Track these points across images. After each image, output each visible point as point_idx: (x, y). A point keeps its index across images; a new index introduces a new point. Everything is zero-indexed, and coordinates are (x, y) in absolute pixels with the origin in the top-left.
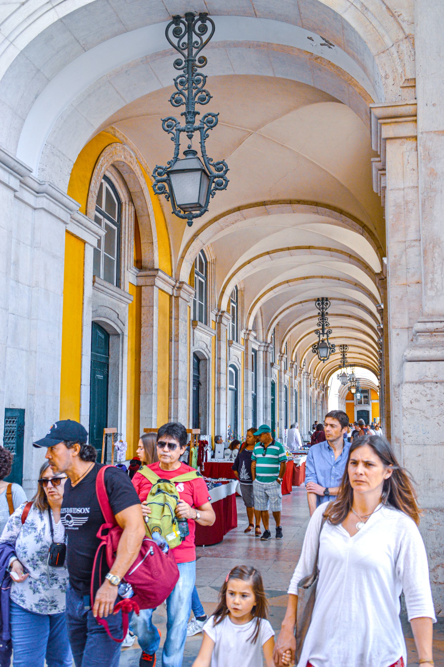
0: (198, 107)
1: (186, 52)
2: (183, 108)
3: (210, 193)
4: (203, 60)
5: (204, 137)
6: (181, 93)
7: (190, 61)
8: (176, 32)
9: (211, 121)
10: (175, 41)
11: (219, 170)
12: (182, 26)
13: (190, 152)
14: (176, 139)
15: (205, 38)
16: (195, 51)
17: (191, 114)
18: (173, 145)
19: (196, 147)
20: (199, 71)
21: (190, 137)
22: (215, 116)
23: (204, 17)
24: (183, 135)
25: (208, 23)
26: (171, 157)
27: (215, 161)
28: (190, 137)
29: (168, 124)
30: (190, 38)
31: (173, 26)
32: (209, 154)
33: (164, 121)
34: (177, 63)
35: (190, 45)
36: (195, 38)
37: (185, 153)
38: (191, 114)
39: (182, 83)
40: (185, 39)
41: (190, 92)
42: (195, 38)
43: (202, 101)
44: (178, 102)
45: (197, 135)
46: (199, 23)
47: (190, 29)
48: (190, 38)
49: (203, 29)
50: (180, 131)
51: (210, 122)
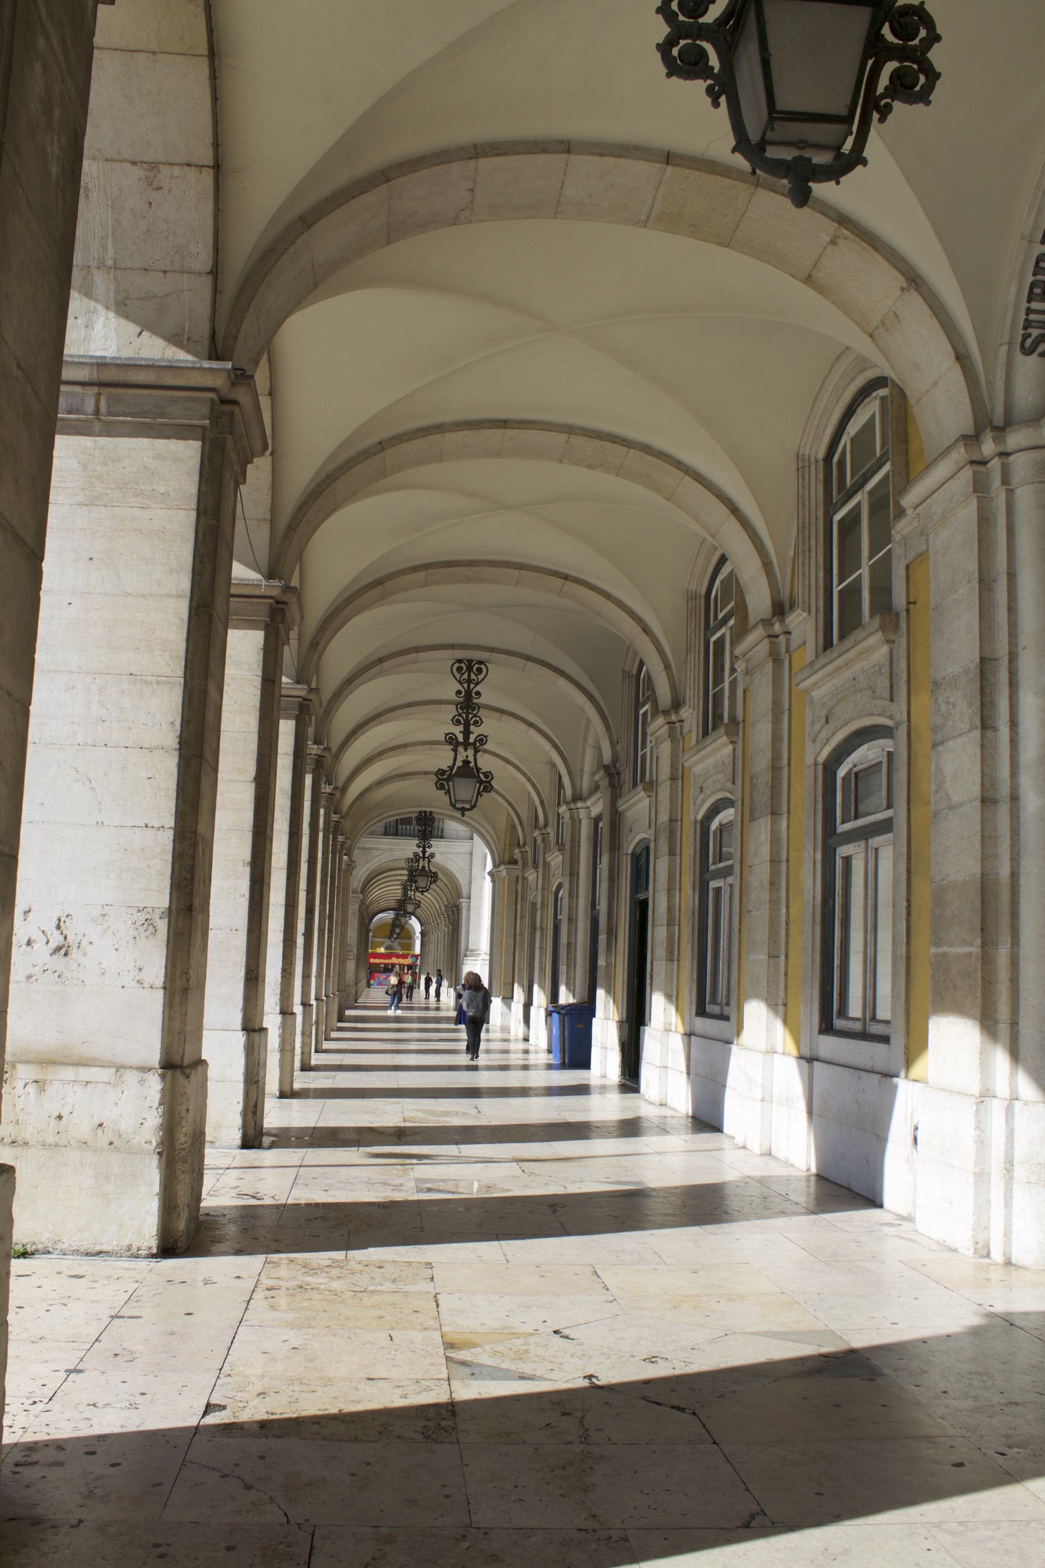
0: (472, 728)
1: (465, 685)
2: (461, 728)
4: (478, 693)
5: (476, 751)
6: (460, 715)
7: (468, 692)
8: (459, 669)
9: (482, 740)
10: (458, 676)
11: (486, 777)
12: (463, 665)
14: (455, 750)
15: (481, 677)
16: (472, 686)
17: (467, 733)
18: (452, 753)
19: (471, 758)
20: (475, 701)
21: (466, 750)
22: (486, 737)
23: (480, 662)
24: (461, 749)
25: (483, 666)
26: (450, 763)
27: (484, 770)
28: (466, 750)
29: (451, 740)
30: (469, 675)
31: (457, 665)
32: (479, 766)
33: (447, 735)
34: (459, 692)
35: (469, 681)
36: (473, 676)
38: (467, 733)
39: (462, 708)
40: (465, 676)
41: (467, 716)
42: (473, 676)
43: (476, 722)
44: (458, 722)
46: (477, 666)
47: (470, 669)
48: (469, 675)
49: (480, 671)
50: (458, 744)
51: (482, 740)
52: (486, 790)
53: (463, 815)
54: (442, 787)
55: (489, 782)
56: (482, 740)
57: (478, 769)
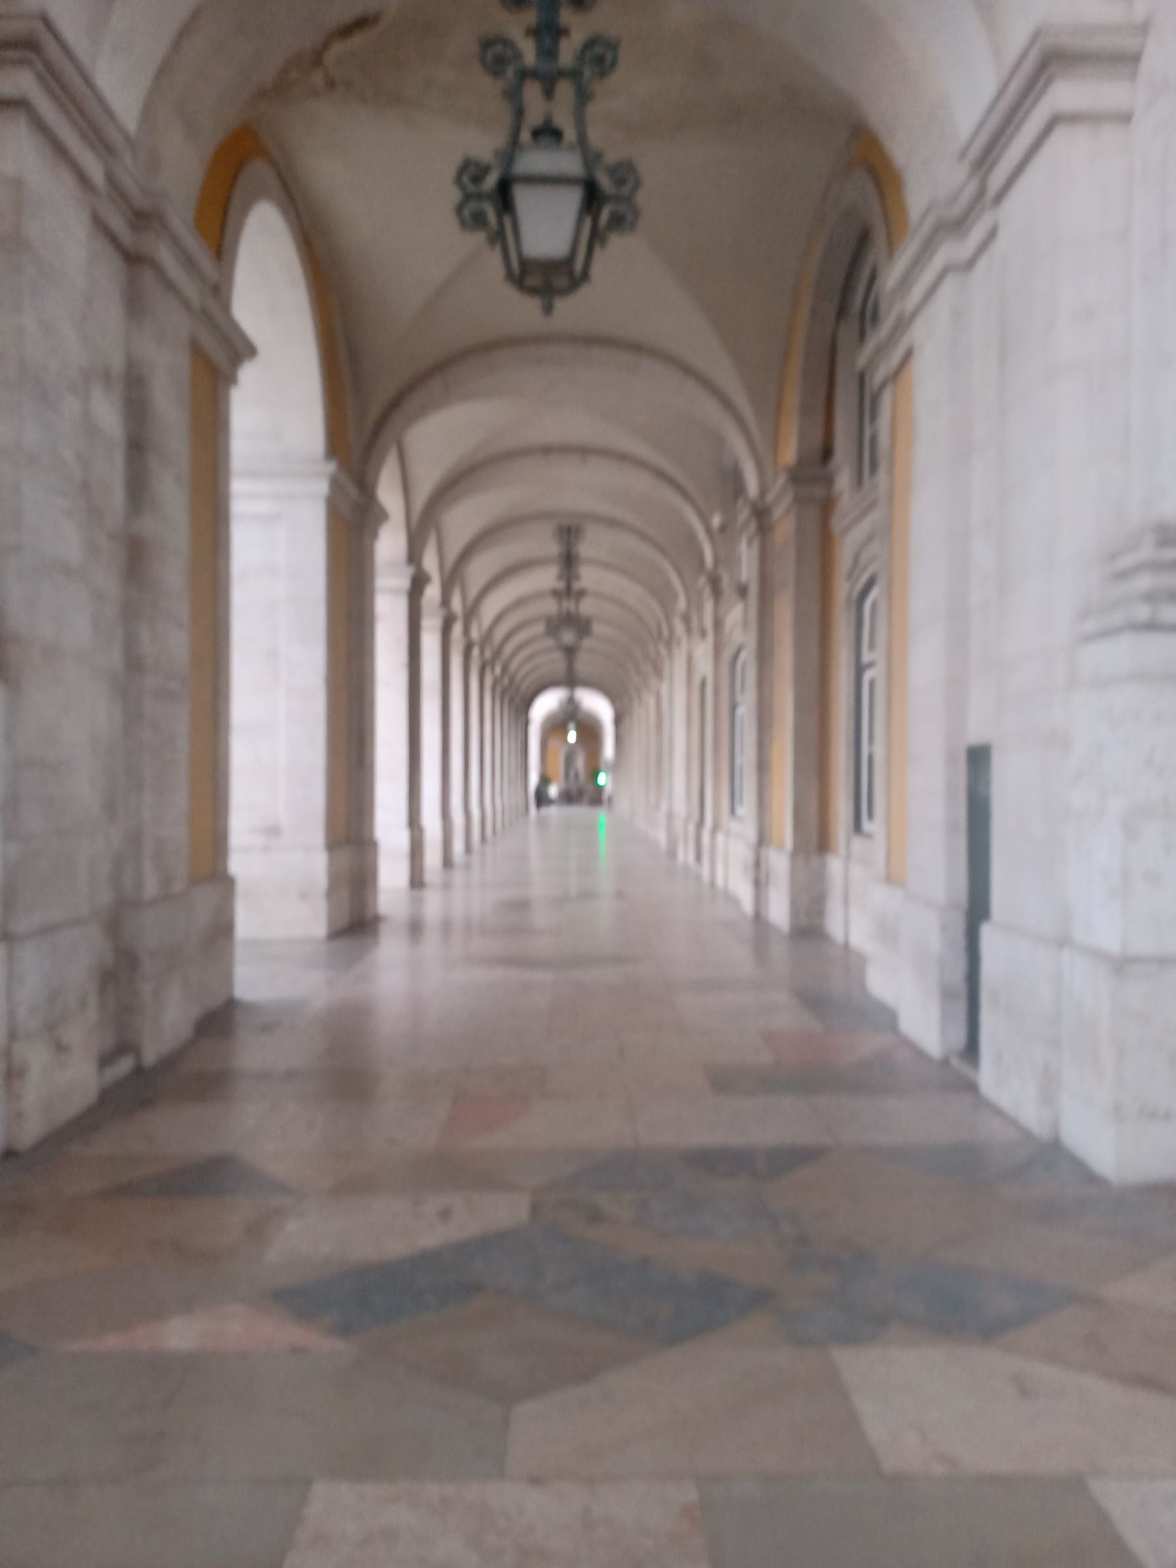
0: (567, 16)
2: (530, 17)
3: (597, 237)
5: (583, 97)
9: (601, 56)
11: (620, 182)
13: (548, 133)
14: (514, 96)
17: (548, 33)
19: (564, 121)
21: (549, 93)
27: (612, 156)
28: (549, 93)
29: (494, 55)
37: (536, 134)
38: (548, 33)
45: (565, 90)
52: (618, 222)
53: (548, 309)
54: (478, 220)
55: (628, 200)
56: (600, 60)
57: (591, 158)
